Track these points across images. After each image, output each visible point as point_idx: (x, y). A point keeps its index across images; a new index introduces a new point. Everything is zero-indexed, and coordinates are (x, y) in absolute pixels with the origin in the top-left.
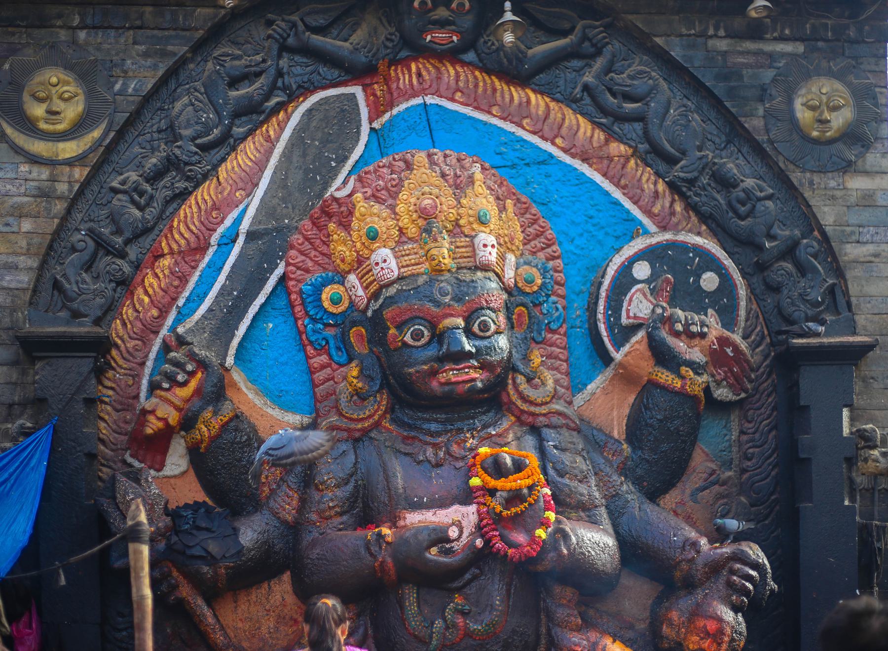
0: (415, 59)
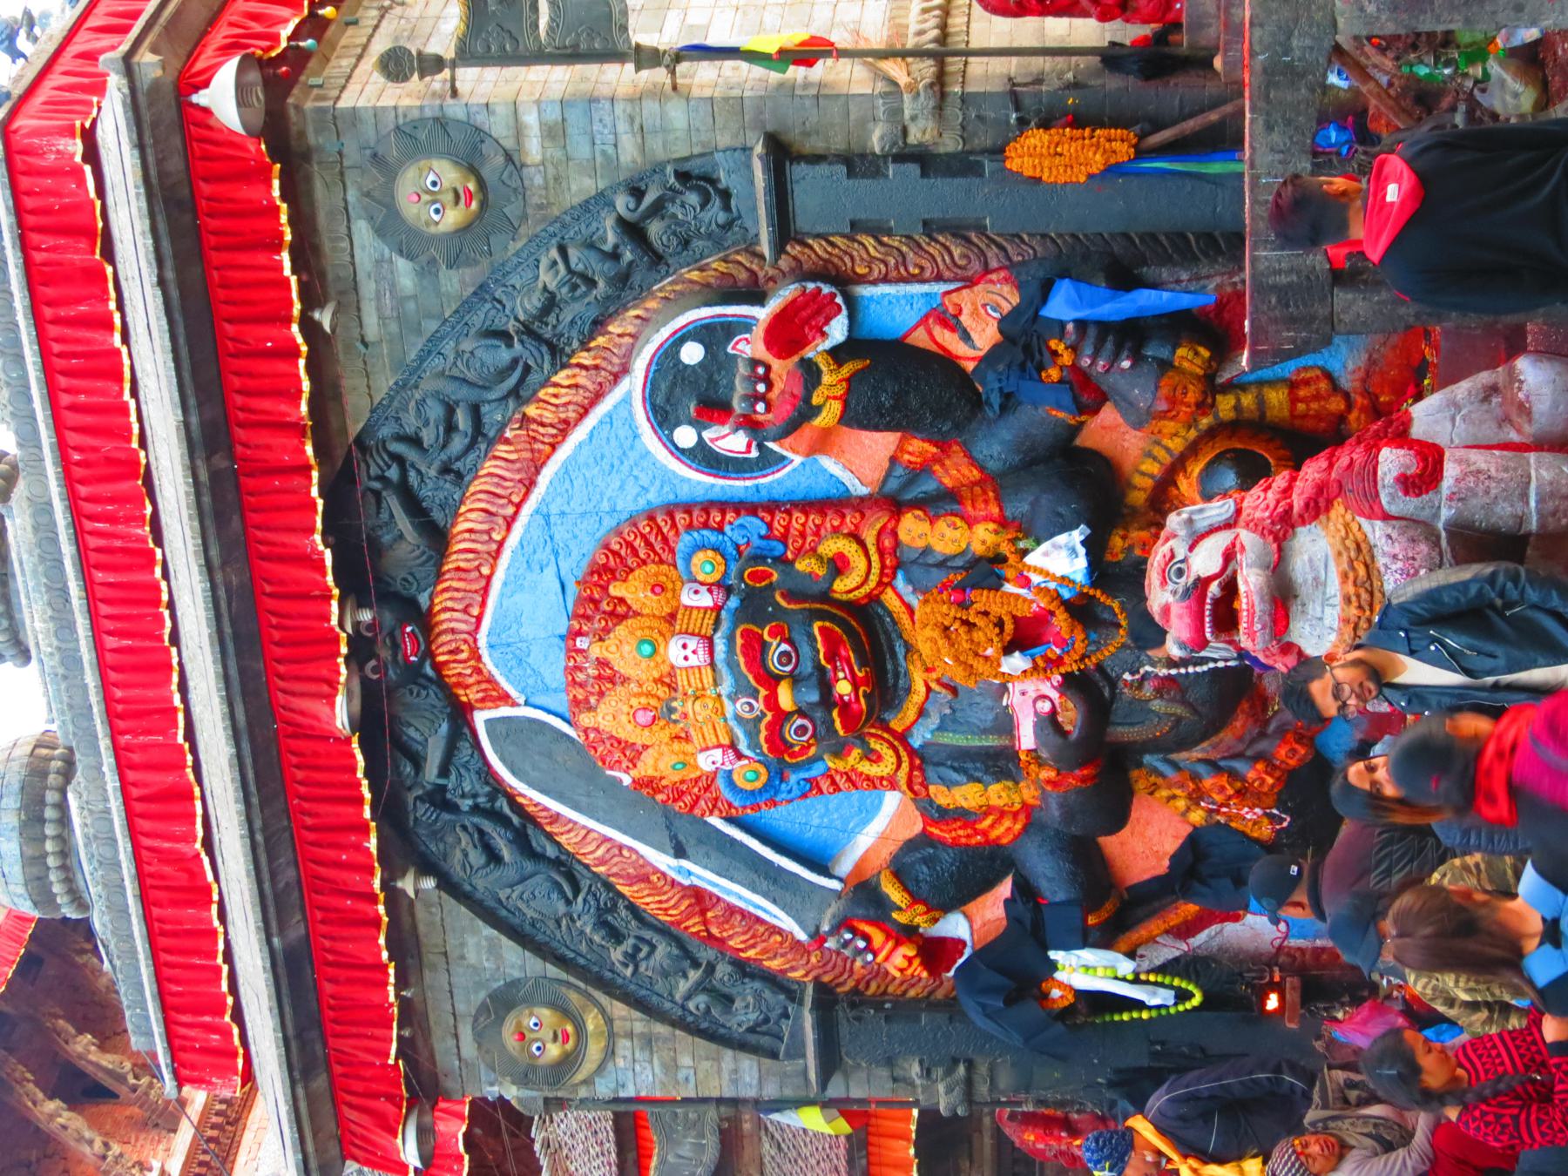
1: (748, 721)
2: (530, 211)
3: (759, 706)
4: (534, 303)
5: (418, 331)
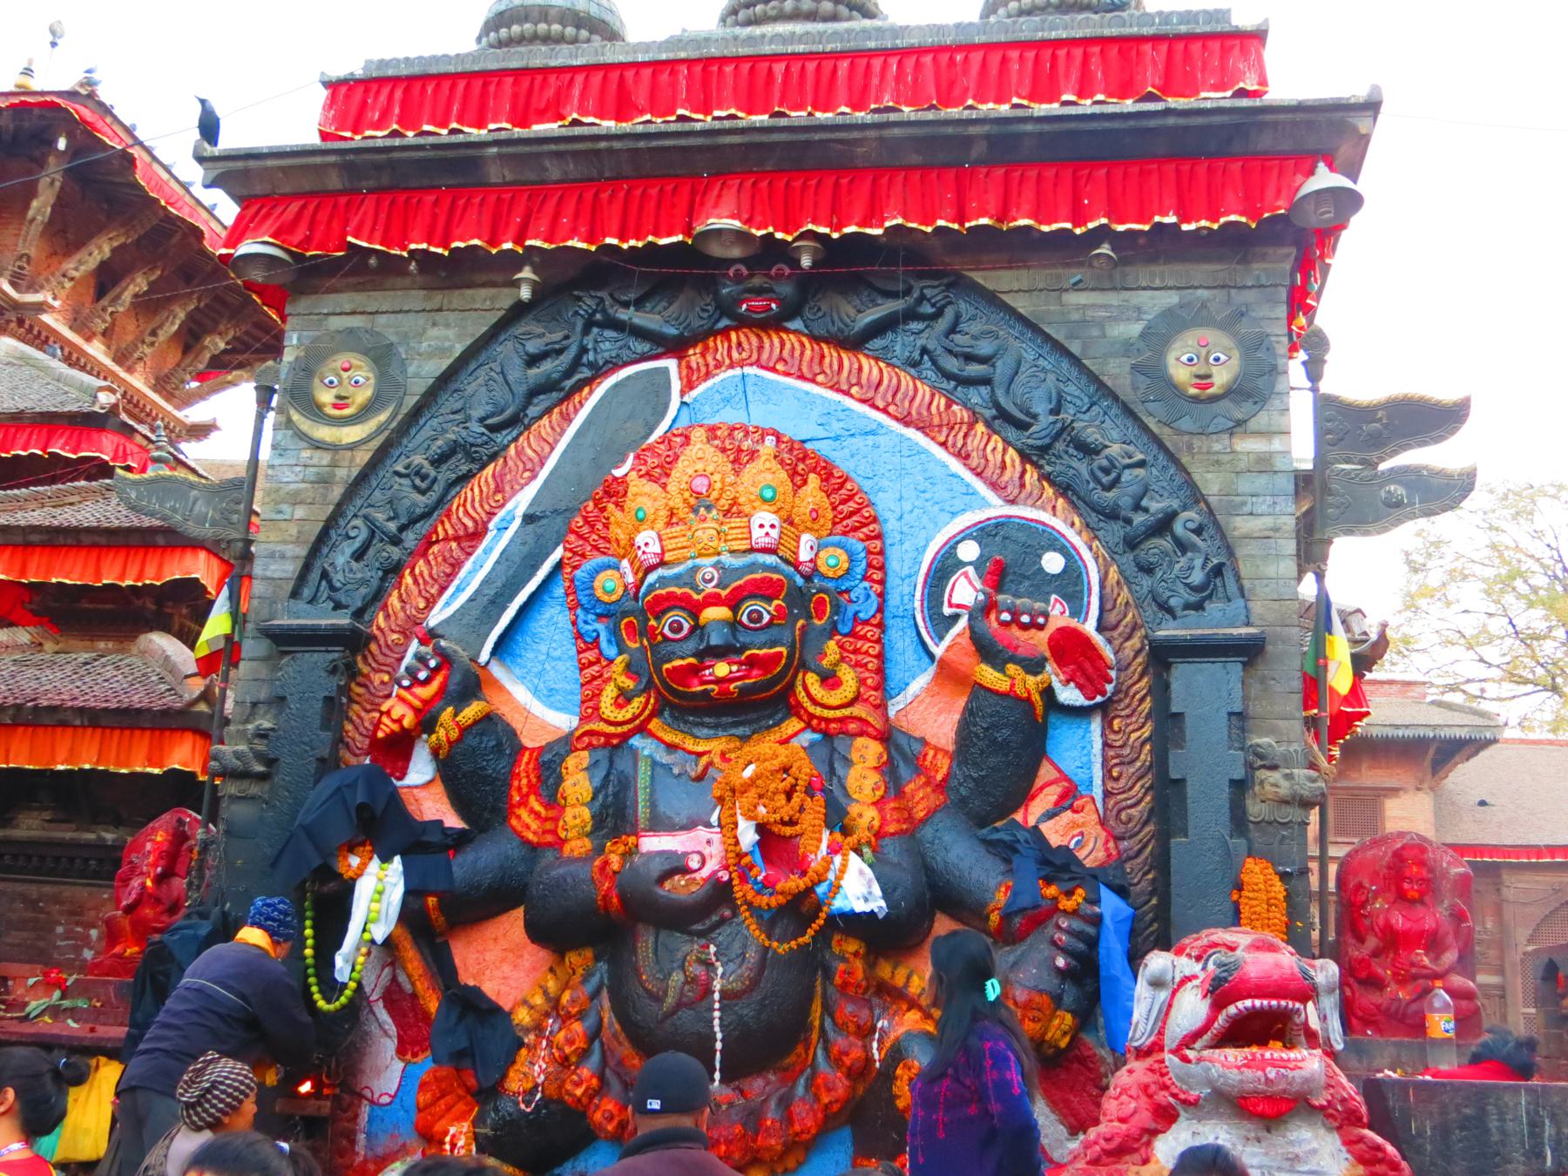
0: (736, 329)
1: (693, 577)
2: (1186, 438)
3: (710, 588)
4: (1092, 436)
5: (1070, 337)
